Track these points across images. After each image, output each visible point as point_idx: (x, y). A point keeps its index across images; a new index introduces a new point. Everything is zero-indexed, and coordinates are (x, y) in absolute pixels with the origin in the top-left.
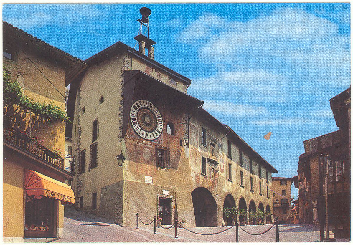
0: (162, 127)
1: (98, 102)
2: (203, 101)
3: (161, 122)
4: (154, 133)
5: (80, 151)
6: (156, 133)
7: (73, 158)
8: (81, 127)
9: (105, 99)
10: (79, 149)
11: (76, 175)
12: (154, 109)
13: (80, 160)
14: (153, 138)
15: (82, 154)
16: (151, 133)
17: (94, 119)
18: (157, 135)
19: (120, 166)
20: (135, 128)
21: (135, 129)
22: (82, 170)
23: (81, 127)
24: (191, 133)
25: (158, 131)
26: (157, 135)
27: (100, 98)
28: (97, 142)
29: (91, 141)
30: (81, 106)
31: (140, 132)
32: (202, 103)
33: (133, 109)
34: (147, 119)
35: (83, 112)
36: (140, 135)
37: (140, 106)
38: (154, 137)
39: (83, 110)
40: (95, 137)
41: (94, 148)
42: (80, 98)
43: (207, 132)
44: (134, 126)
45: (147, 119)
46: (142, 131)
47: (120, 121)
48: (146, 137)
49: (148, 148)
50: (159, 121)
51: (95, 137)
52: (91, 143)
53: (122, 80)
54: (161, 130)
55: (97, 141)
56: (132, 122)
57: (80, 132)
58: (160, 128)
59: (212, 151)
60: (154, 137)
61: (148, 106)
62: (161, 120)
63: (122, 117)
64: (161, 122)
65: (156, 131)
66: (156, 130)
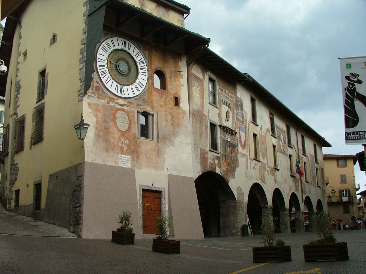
0: (146, 78)
1: (49, 42)
2: (210, 39)
3: (144, 69)
4: (133, 86)
5: (17, 116)
6: (136, 87)
7: (6, 128)
8: (20, 80)
9: (58, 39)
10: (16, 114)
11: (10, 156)
12: (134, 51)
13: (17, 129)
14: (131, 95)
15: (22, 122)
16: (129, 88)
17: (40, 68)
18: (138, 90)
19: (79, 139)
20: (104, 80)
21: (104, 82)
22: (20, 148)
23: (20, 80)
24: (192, 87)
25: (140, 83)
26: (138, 90)
27: (50, 37)
28: (44, 104)
29: (36, 101)
30: (22, 50)
31: (112, 85)
32: (207, 41)
33: (100, 51)
34: (123, 67)
35: (25, 58)
36: (112, 90)
37: (112, 46)
38: (134, 93)
39: (25, 54)
40: (42, 94)
41: (40, 112)
42: (20, 38)
43: (217, 83)
44: (101, 77)
45: (123, 67)
46: (115, 84)
47: (80, 69)
48: (121, 93)
49: (123, 110)
50: (141, 69)
51: (42, 94)
52: (36, 105)
53: (86, 10)
54: (144, 83)
55: (43, 101)
56: (99, 71)
57: (18, 88)
58: (143, 78)
59: (226, 113)
60: (134, 93)
61: (124, 46)
62: (146, 67)
63: (85, 54)
64: (144, 69)
65: (136, 84)
66: (137, 82)
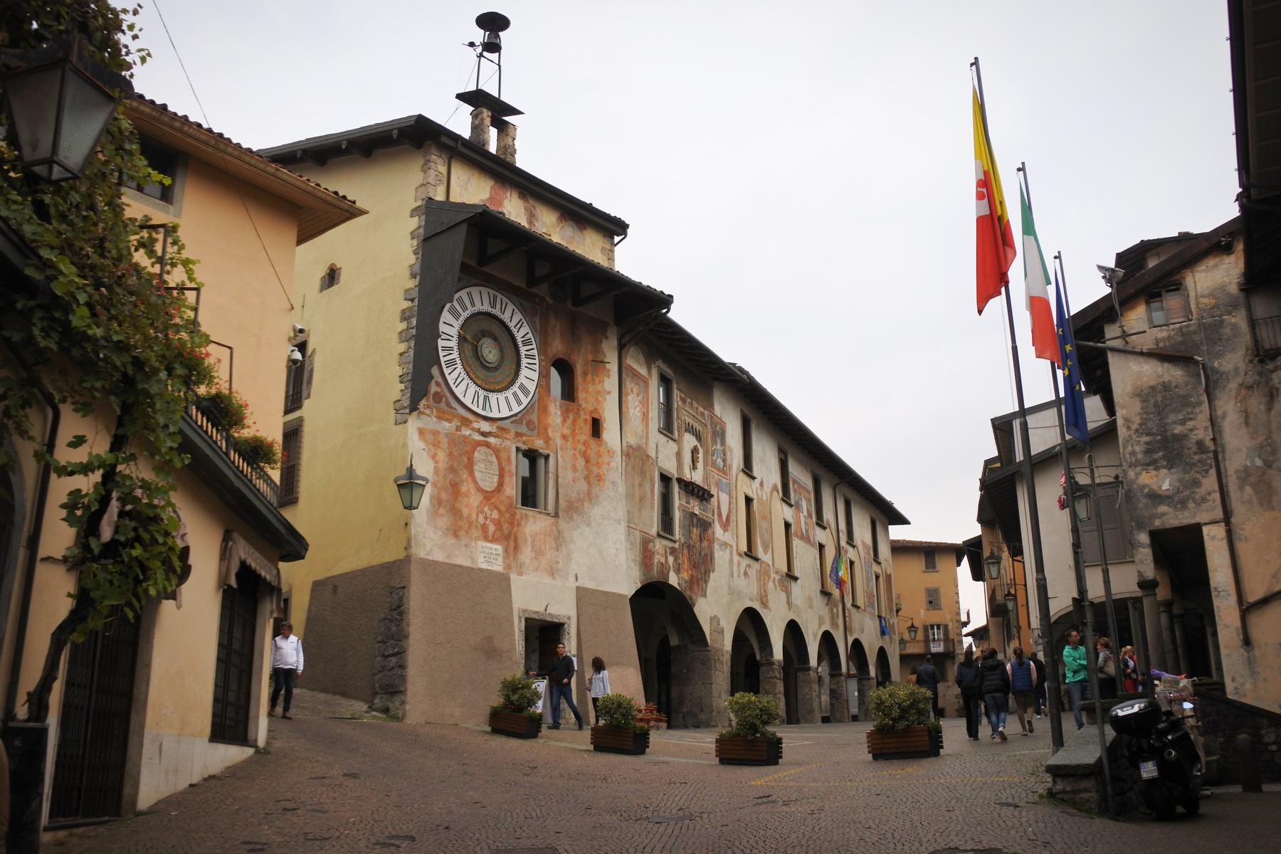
0: (535, 376)
1: (317, 283)
4: (509, 393)
6: (515, 394)
9: (344, 277)
12: (512, 317)
14: (505, 413)
16: (501, 396)
18: (519, 403)
19: (405, 508)
20: (450, 379)
21: (451, 383)
24: (627, 394)
25: (522, 387)
26: (519, 403)
27: (322, 271)
31: (466, 391)
33: (446, 316)
34: (490, 352)
36: (467, 401)
44: (446, 371)
46: (473, 388)
47: (401, 354)
48: (484, 408)
49: (488, 445)
50: (527, 356)
54: (531, 387)
58: (529, 376)
59: (692, 452)
61: (494, 306)
62: (535, 352)
65: (515, 388)
